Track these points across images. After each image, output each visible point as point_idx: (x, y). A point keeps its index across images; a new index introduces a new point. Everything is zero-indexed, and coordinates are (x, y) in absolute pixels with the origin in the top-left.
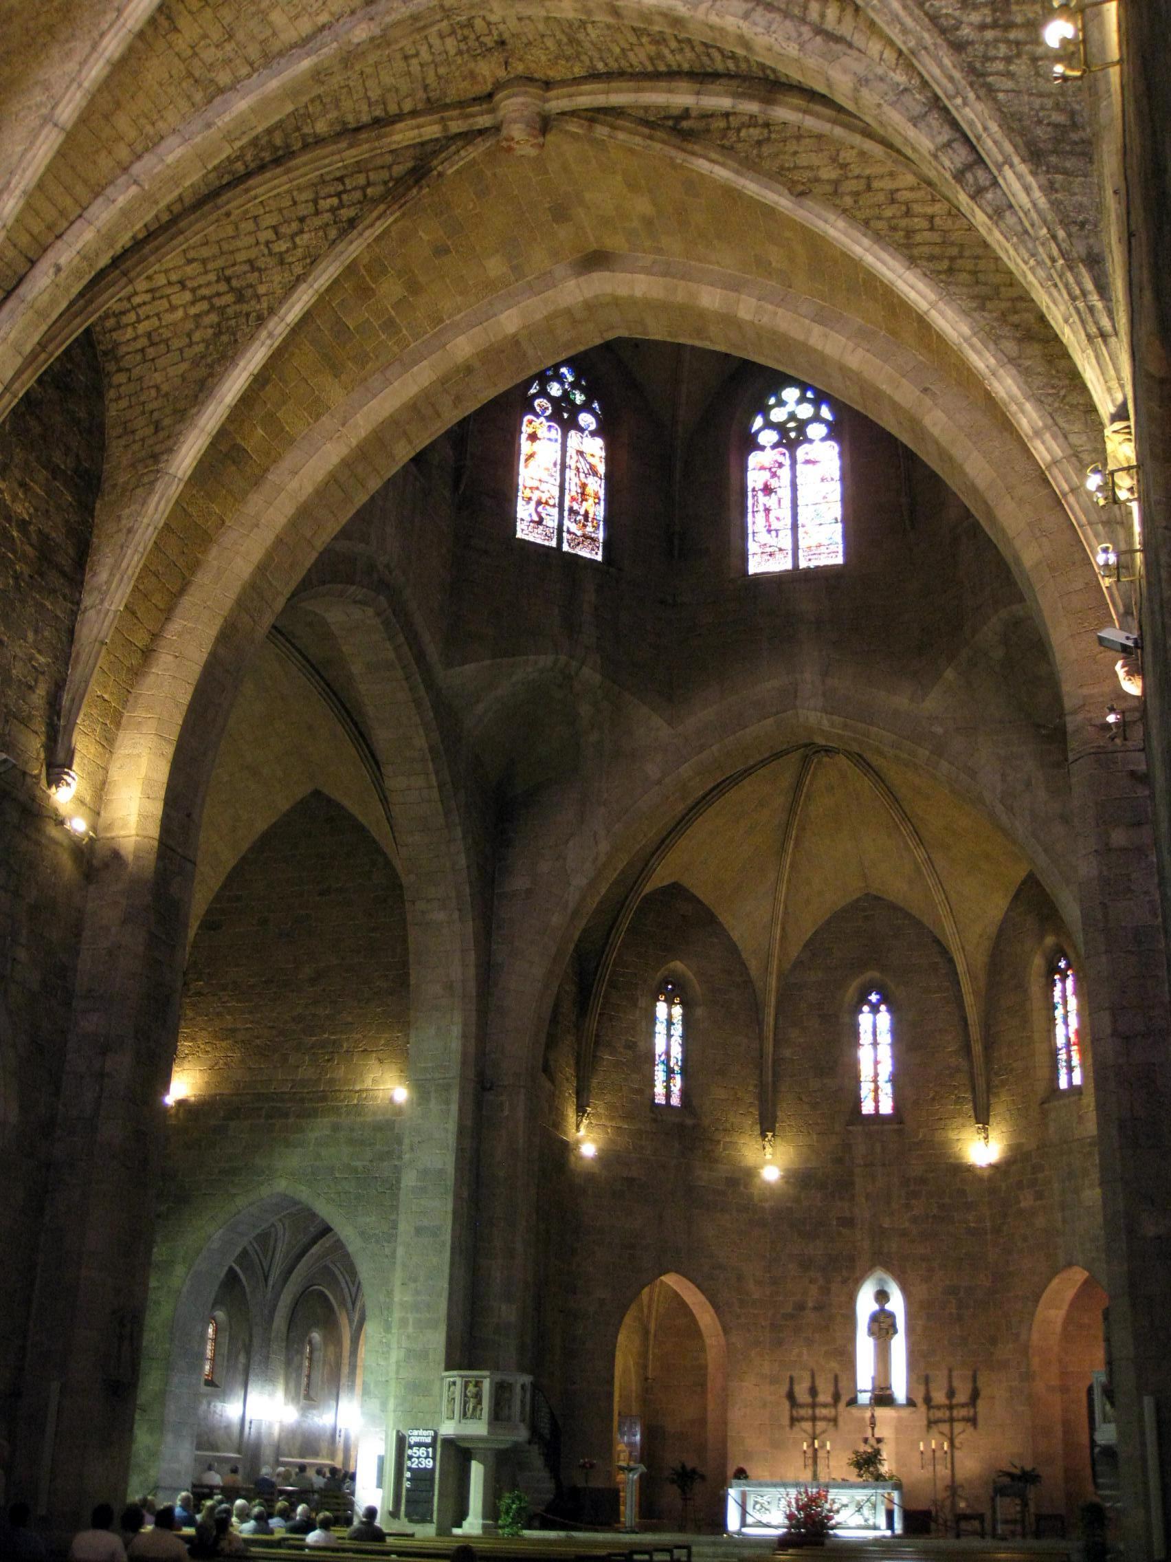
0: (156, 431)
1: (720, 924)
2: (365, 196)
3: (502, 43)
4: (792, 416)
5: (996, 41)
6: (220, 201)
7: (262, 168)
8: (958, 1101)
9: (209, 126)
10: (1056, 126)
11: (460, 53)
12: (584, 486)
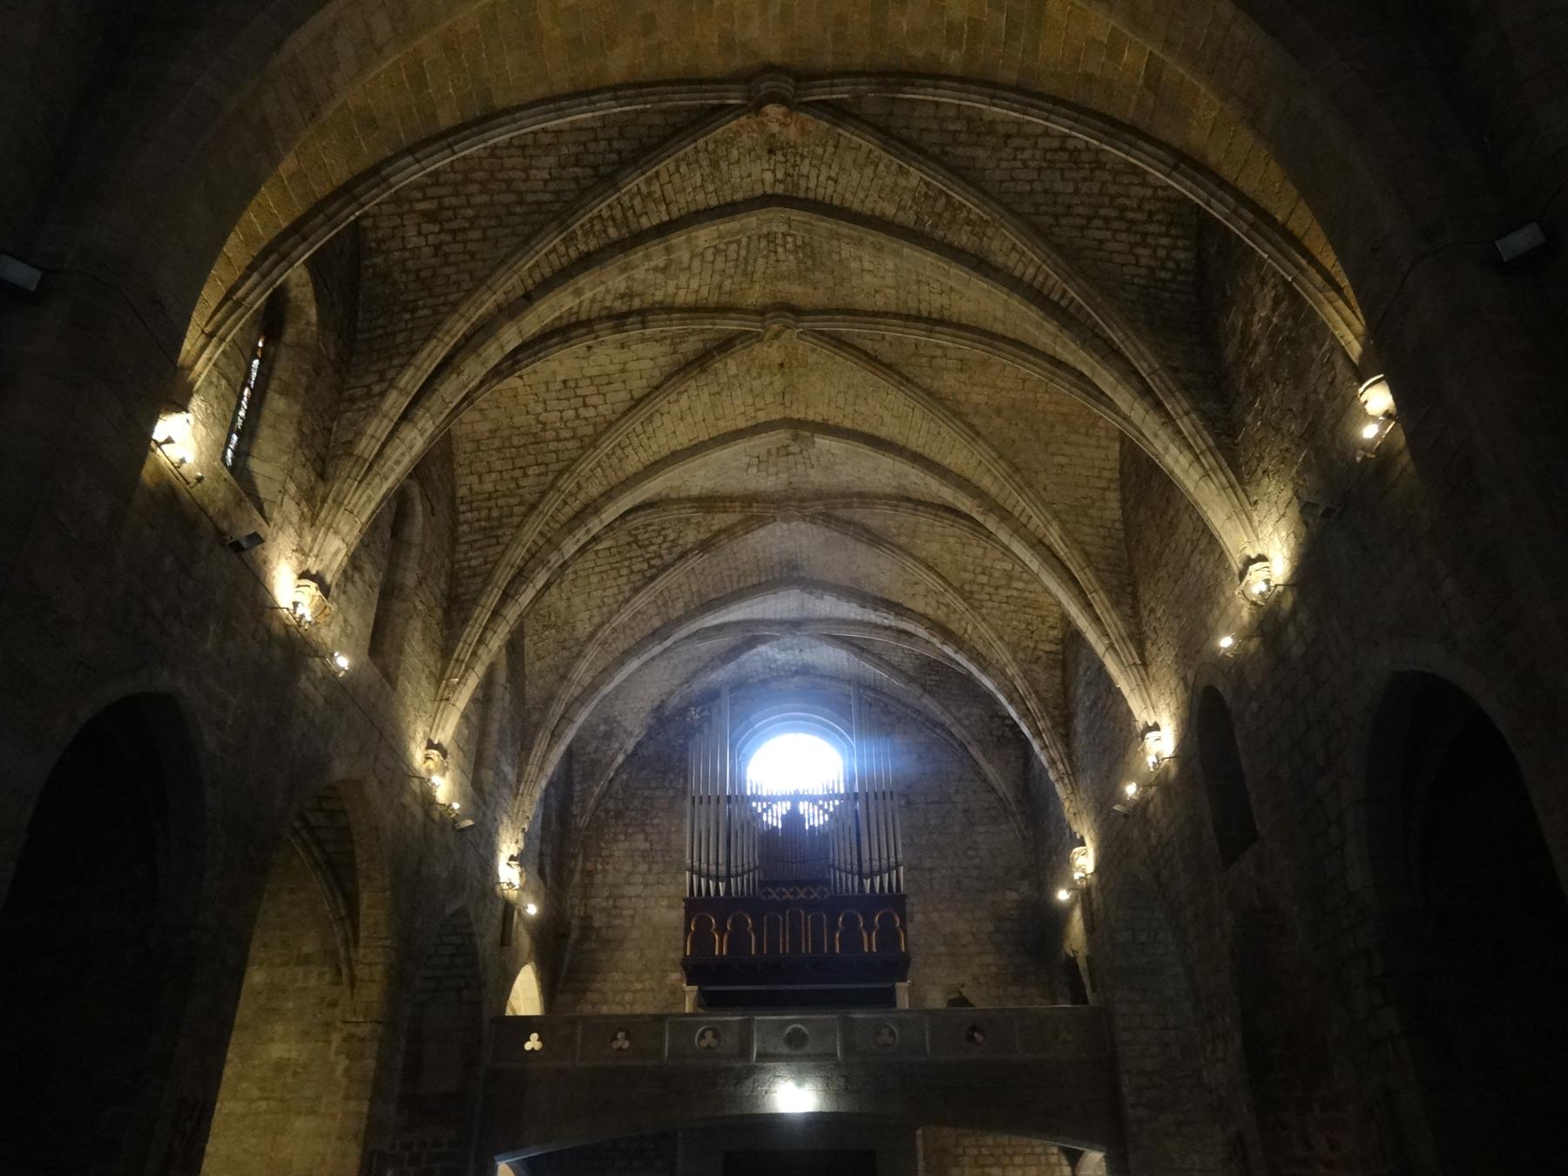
3: (771, 151)
11: (802, 157)
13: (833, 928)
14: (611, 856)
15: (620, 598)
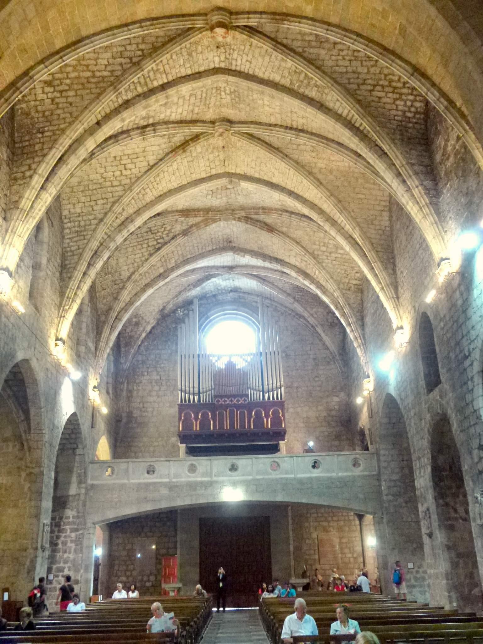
11: (234, 50)
13: (250, 417)
14: (141, 382)
15: (143, 259)
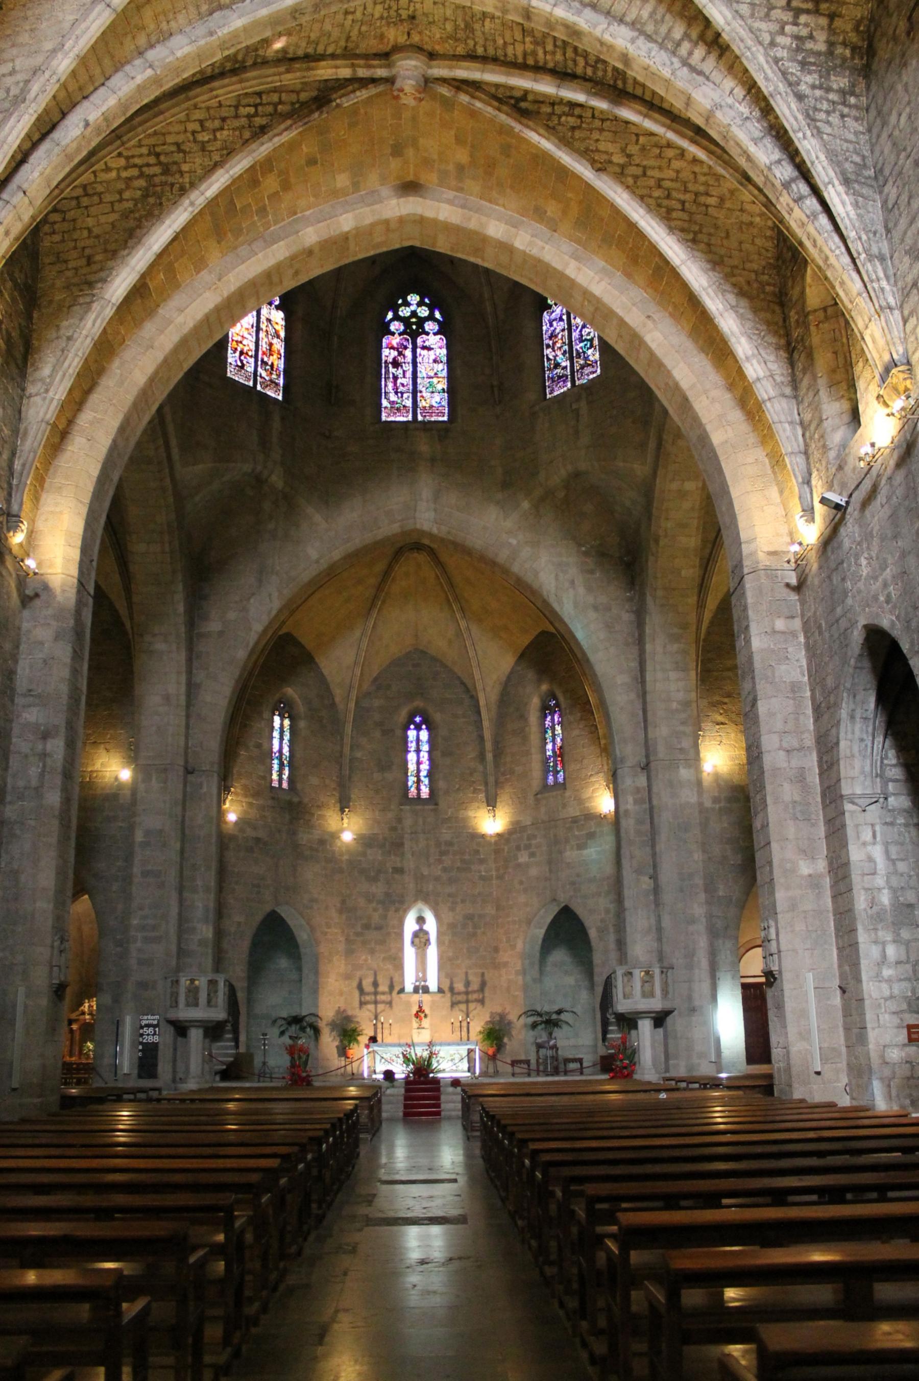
0: (89, 264)
1: (316, 664)
2: (276, 110)
3: (413, 18)
4: (414, 314)
5: (821, 97)
6: (191, 93)
7: (222, 75)
8: (475, 791)
9: (211, 34)
10: (856, 164)
11: (382, 18)
12: (271, 345)
